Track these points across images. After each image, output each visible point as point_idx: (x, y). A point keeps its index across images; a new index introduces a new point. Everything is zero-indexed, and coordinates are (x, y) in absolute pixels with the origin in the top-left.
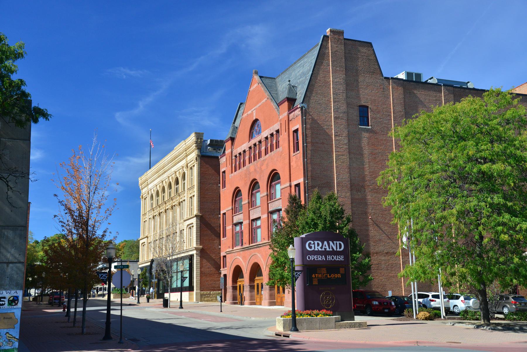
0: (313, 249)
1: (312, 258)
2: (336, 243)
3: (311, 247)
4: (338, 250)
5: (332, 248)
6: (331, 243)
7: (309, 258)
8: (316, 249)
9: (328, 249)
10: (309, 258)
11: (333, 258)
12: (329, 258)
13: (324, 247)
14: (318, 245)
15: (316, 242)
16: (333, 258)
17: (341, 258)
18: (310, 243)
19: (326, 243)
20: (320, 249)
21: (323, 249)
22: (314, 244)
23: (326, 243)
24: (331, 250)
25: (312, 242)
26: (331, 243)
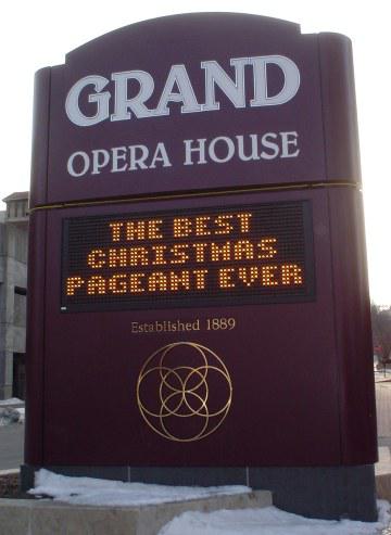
0: (102, 114)
1: (94, 162)
2: (249, 70)
3: (88, 109)
4: (261, 99)
5: (220, 95)
6: (212, 69)
7: (79, 164)
8: (121, 115)
9: (191, 106)
10: (79, 164)
11: (221, 150)
12: (198, 151)
13: (167, 96)
14: (134, 88)
15: (121, 79)
16: (221, 150)
17: (283, 146)
18: (90, 89)
19: (178, 73)
20: (143, 113)
21: (162, 110)
22: (110, 88)
23: (178, 73)
24: (211, 105)
25: (100, 82)
26: (212, 69)
